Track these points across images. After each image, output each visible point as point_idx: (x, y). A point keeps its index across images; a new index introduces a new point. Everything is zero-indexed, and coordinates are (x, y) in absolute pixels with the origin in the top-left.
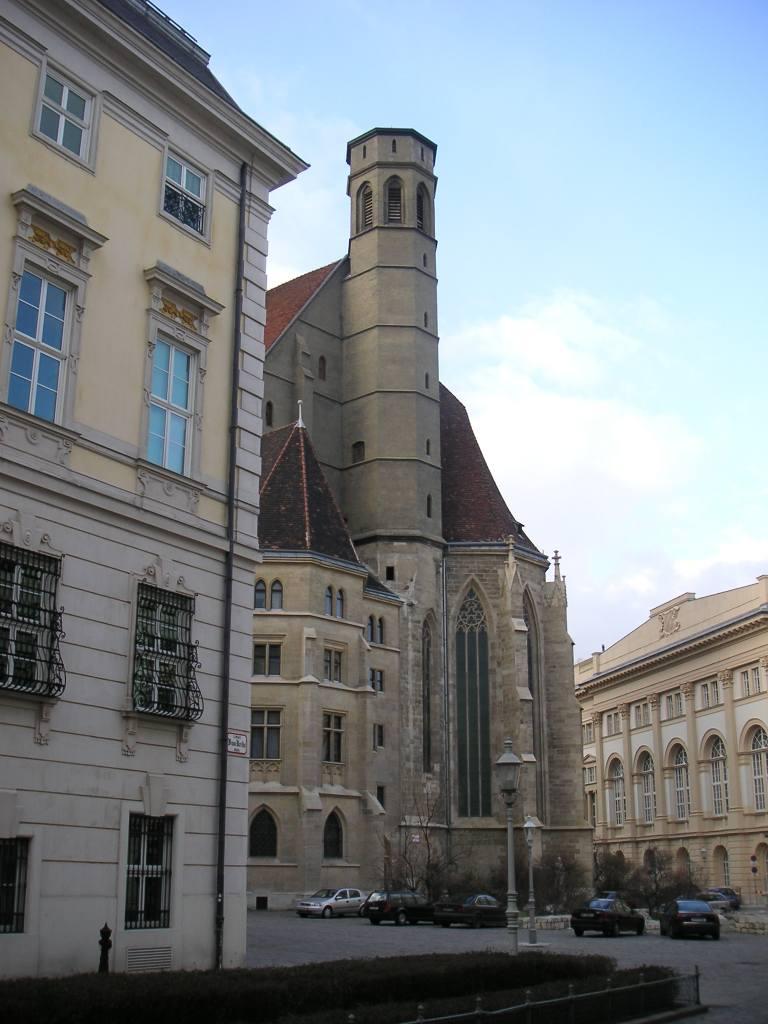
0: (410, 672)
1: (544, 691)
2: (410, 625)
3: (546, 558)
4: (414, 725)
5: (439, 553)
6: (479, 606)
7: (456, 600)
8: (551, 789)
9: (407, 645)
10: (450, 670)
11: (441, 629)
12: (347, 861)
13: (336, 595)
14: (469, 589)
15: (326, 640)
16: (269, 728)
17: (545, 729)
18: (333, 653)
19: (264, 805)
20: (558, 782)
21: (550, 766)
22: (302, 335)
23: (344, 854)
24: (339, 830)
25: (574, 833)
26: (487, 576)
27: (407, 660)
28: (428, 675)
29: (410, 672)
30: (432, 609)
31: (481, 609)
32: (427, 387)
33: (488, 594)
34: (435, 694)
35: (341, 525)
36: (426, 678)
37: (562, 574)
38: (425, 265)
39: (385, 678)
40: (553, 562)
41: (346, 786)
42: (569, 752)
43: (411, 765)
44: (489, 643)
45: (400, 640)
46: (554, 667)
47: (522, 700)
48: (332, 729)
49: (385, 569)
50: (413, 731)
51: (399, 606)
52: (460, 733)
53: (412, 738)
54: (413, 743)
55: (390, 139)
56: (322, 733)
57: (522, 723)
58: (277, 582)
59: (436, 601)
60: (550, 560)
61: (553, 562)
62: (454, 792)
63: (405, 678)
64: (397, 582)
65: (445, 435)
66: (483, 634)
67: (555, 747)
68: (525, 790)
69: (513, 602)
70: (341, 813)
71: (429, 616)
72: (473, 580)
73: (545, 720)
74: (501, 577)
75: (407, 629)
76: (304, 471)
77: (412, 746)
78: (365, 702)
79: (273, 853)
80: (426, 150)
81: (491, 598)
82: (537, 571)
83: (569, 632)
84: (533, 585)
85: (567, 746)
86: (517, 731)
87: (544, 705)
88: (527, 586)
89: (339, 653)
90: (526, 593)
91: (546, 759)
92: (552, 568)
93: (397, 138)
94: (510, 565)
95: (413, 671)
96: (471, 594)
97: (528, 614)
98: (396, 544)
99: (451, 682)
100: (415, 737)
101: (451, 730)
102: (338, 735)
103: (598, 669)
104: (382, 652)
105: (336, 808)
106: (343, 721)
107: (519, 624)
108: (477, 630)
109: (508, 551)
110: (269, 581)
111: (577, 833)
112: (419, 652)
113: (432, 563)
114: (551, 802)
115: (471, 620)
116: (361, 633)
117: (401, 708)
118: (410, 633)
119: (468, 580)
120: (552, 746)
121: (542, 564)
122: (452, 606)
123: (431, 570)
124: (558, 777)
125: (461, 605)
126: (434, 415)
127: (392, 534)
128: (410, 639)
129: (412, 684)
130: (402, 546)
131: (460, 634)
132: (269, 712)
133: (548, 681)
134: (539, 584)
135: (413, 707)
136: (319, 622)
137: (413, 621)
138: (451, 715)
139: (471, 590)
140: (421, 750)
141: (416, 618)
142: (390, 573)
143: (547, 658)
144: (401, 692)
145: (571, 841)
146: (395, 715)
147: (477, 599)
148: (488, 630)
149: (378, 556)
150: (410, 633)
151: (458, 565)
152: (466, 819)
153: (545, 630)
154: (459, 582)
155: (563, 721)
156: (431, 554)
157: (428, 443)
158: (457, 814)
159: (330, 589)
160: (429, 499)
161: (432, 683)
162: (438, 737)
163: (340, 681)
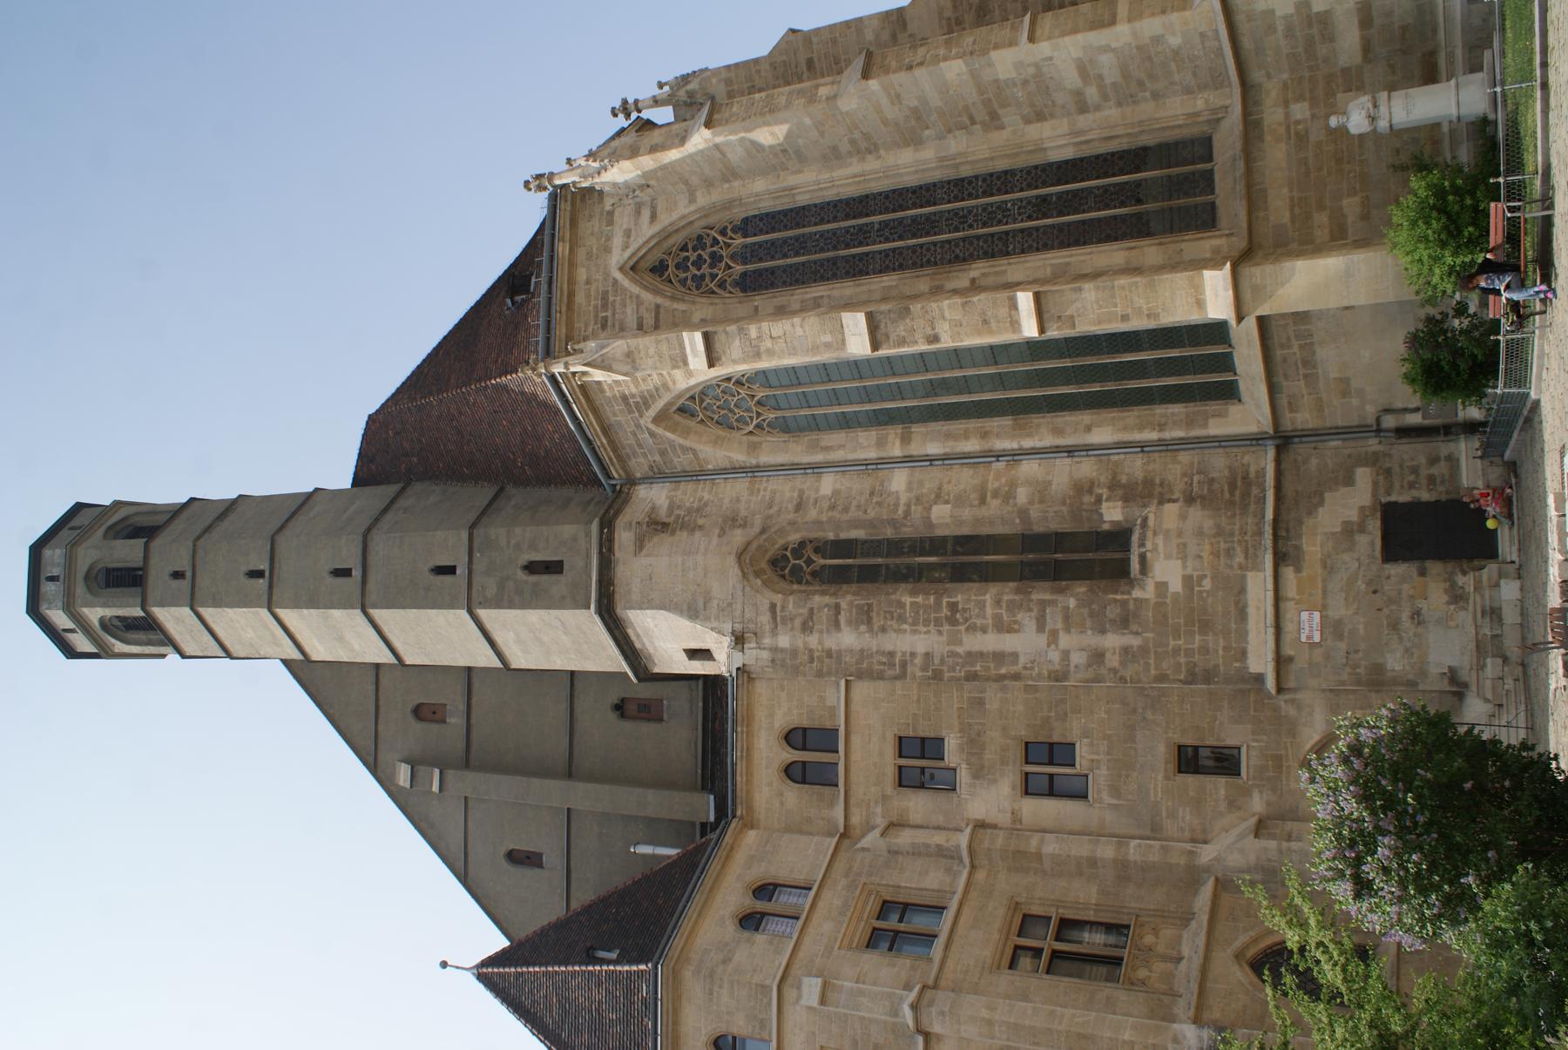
1: (855, 167)
2: (784, 641)
4: (1010, 630)
5: (624, 537)
6: (703, 393)
9: (829, 654)
10: (872, 454)
11: (784, 489)
20: (1092, 93)
21: (1052, 116)
25: (1243, 27)
27: (862, 651)
42: (996, 81)
43: (1112, 641)
53: (1042, 640)
54: (1053, 638)
62: (1173, 420)
67: (994, 116)
72: (657, 420)
73: (928, 153)
75: (794, 652)
77: (1065, 641)
82: (590, 227)
84: (617, 257)
85: (981, 92)
88: (621, 269)
91: (1037, 132)
95: (883, 630)
99: (897, 452)
100: (1041, 627)
101: (1015, 445)
104: (856, 740)
112: (837, 607)
114: (1156, 96)
117: (972, 677)
118: (800, 643)
119: (659, 431)
120: (994, 121)
124: (1078, 94)
128: (813, 640)
131: (786, 427)
133: (833, 156)
135: (972, 629)
137: (774, 633)
138: (972, 445)
140: (1072, 603)
141: (765, 618)
145: (1272, 29)
146: (993, 698)
147: (692, 398)
151: (639, 451)
152: (1242, 386)
153: (709, 184)
154: (673, 447)
155: (915, 111)
156: (632, 569)
158: (1234, 410)
160: (532, 568)
161: (907, 532)
162: (1034, 513)
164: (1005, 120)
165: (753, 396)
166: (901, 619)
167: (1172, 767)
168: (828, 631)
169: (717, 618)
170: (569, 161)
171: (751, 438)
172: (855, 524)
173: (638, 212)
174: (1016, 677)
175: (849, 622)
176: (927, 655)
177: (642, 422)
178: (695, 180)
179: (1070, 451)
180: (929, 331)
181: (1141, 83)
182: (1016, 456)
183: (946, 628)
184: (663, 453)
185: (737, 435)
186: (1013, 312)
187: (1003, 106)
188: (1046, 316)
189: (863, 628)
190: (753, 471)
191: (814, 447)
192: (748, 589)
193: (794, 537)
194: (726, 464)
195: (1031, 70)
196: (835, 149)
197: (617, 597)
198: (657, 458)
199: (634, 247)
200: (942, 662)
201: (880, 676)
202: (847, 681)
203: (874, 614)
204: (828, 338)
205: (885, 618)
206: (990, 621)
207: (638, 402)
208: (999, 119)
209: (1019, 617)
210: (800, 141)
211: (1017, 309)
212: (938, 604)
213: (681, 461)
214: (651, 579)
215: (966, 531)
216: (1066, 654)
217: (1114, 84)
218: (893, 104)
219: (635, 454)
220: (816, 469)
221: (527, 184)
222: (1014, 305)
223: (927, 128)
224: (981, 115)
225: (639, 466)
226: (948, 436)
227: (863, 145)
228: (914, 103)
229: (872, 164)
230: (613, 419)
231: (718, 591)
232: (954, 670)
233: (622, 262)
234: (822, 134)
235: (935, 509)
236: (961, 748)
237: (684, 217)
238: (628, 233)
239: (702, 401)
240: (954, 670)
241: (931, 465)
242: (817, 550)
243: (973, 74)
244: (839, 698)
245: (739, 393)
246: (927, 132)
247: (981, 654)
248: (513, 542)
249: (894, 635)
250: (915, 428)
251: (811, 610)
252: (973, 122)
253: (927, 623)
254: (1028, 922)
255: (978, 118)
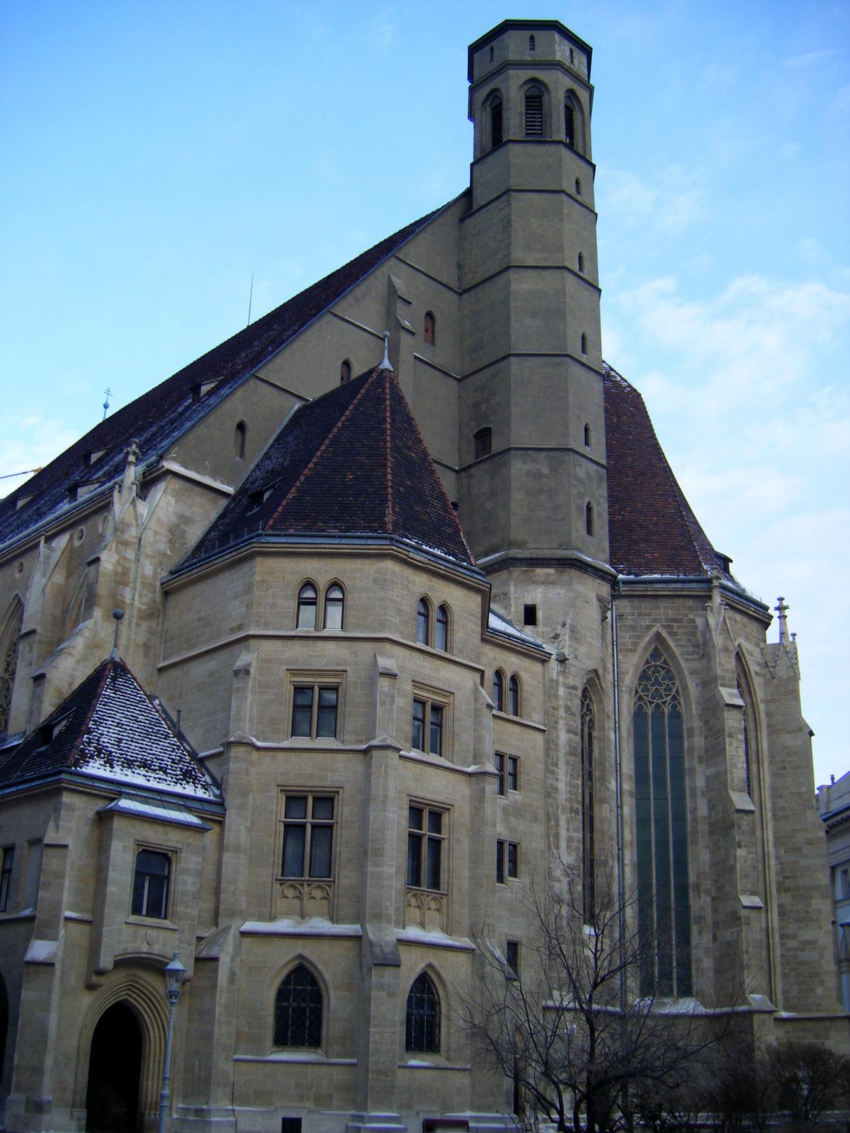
0: (562, 764)
2: (562, 691)
3: (767, 608)
4: (568, 846)
5: (605, 589)
6: (668, 671)
7: (632, 665)
8: (782, 956)
9: (556, 722)
12: (448, 1059)
13: (435, 614)
14: (653, 646)
15: (416, 684)
16: (314, 826)
17: (773, 862)
18: (428, 707)
19: (301, 956)
20: (792, 944)
21: (781, 920)
22: (399, 277)
23: (443, 1047)
24: (434, 1005)
25: (821, 1025)
26: (679, 627)
27: (557, 745)
28: (590, 773)
29: (562, 764)
30: (595, 671)
31: (672, 678)
32: (584, 351)
33: (682, 654)
34: (603, 801)
35: (446, 511)
36: (588, 776)
37: (790, 631)
38: (578, 191)
39: (521, 769)
40: (776, 614)
41: (447, 930)
42: (811, 897)
44: (685, 726)
45: (546, 713)
46: (784, 768)
47: (739, 811)
48: (425, 831)
49: (522, 610)
50: (568, 856)
51: (544, 659)
52: (642, 866)
55: (527, 34)
56: (406, 837)
57: (739, 847)
58: (336, 585)
59: (603, 661)
60: (771, 611)
61: (776, 614)
63: (552, 772)
64: (540, 628)
65: (611, 429)
66: (676, 715)
67: (787, 890)
68: (747, 952)
69: (725, 665)
70: (438, 975)
71: (590, 681)
72: (658, 635)
74: (701, 628)
75: (557, 697)
76: (389, 426)
78: (483, 790)
79: (314, 1040)
80: (577, 53)
81: (686, 660)
82: (753, 627)
83: (804, 715)
84: (747, 646)
86: (732, 861)
87: (770, 826)
88: (739, 645)
89: (437, 709)
90: (739, 657)
91: (775, 909)
92: (775, 623)
93: (536, 33)
94: (715, 610)
95: (567, 763)
96: (656, 654)
97: (743, 682)
98: (539, 571)
101: (627, 861)
102: (436, 844)
103: (828, 808)
104: (517, 729)
105: (430, 966)
106: (445, 819)
107: (731, 695)
108: (666, 710)
109: (710, 589)
110: (322, 582)
111: (827, 1024)
112: (575, 734)
113: (595, 600)
114: (785, 976)
115: (657, 694)
116: (478, 681)
117: (549, 820)
118: (561, 703)
121: (759, 615)
122: (623, 673)
123: (593, 611)
124: (794, 937)
125: (640, 671)
126: (598, 386)
127: (534, 556)
128: (561, 712)
129: (565, 782)
130: (547, 574)
131: (639, 715)
132: (315, 799)
134: (758, 645)
135: (568, 823)
136: (406, 652)
139: (656, 649)
141: (571, 681)
142: (530, 616)
143: (772, 756)
144: (548, 795)
146: (539, 829)
147: (665, 662)
148: (683, 710)
149: (512, 589)
150: (561, 703)
151: (636, 612)
153: (768, 714)
154: (638, 637)
156: (592, 589)
157: (586, 430)
159: (424, 601)
160: (589, 509)
161: (597, 786)
163: (441, 755)
164: (783, 894)
165: (664, 703)
166: (572, 776)
167: (511, 938)
168: (566, 724)
169: (570, 646)
170: (794, 635)
171: (634, 690)
172: (602, 752)
173: (759, 664)
174: (549, 847)
175: (570, 740)
176: (557, 789)
177: (658, 624)
178: (773, 707)
179: (622, 895)
180: (743, 844)
181: (794, 969)
182: (621, 860)
183: (569, 805)
184: (633, 628)
185: (636, 682)
186: (749, 892)
187: (793, 896)
188: (750, 910)
189: (567, 748)
190: (617, 684)
191: (628, 730)
192: (584, 673)
193: (595, 708)
194: (622, 669)
195: (814, 917)
196: (781, 797)
197: (578, 572)
198: (629, 622)
199: (746, 654)
200: (555, 799)
201: (547, 755)
202: (545, 731)
203: (573, 758)
204: (736, 782)
205: (572, 765)
206: (572, 834)
207: (673, 628)
208: (785, 891)
209: (573, 853)
210: (789, 780)
211: (751, 895)
212: (578, 803)
213: (626, 638)
214: (587, 602)
215: (597, 824)
216: (559, 881)
217: (797, 956)
218: (807, 839)
219: (633, 608)
220: (617, 729)
221: (781, 599)
222: (753, 893)
223: (786, 852)
224: (788, 883)
225: (624, 606)
226: (632, 821)
227: (779, 813)
228: (805, 850)
229: (769, 815)
230: (662, 605)
231: (583, 650)
232: (551, 806)
233: (742, 646)
234: (792, 794)
235: (607, 805)
236: (516, 802)
237: (755, 694)
238: (751, 654)
239: (663, 668)
240: (551, 806)
241: (618, 807)
242: (591, 721)
243: (818, 887)
244: (534, 722)
245: (667, 696)
246: (783, 851)
247: (558, 826)
248: (601, 500)
249: (565, 769)
250: (634, 800)
251: (573, 714)
252: (784, 877)
253: (570, 791)
254: (326, 800)
255: (787, 881)
